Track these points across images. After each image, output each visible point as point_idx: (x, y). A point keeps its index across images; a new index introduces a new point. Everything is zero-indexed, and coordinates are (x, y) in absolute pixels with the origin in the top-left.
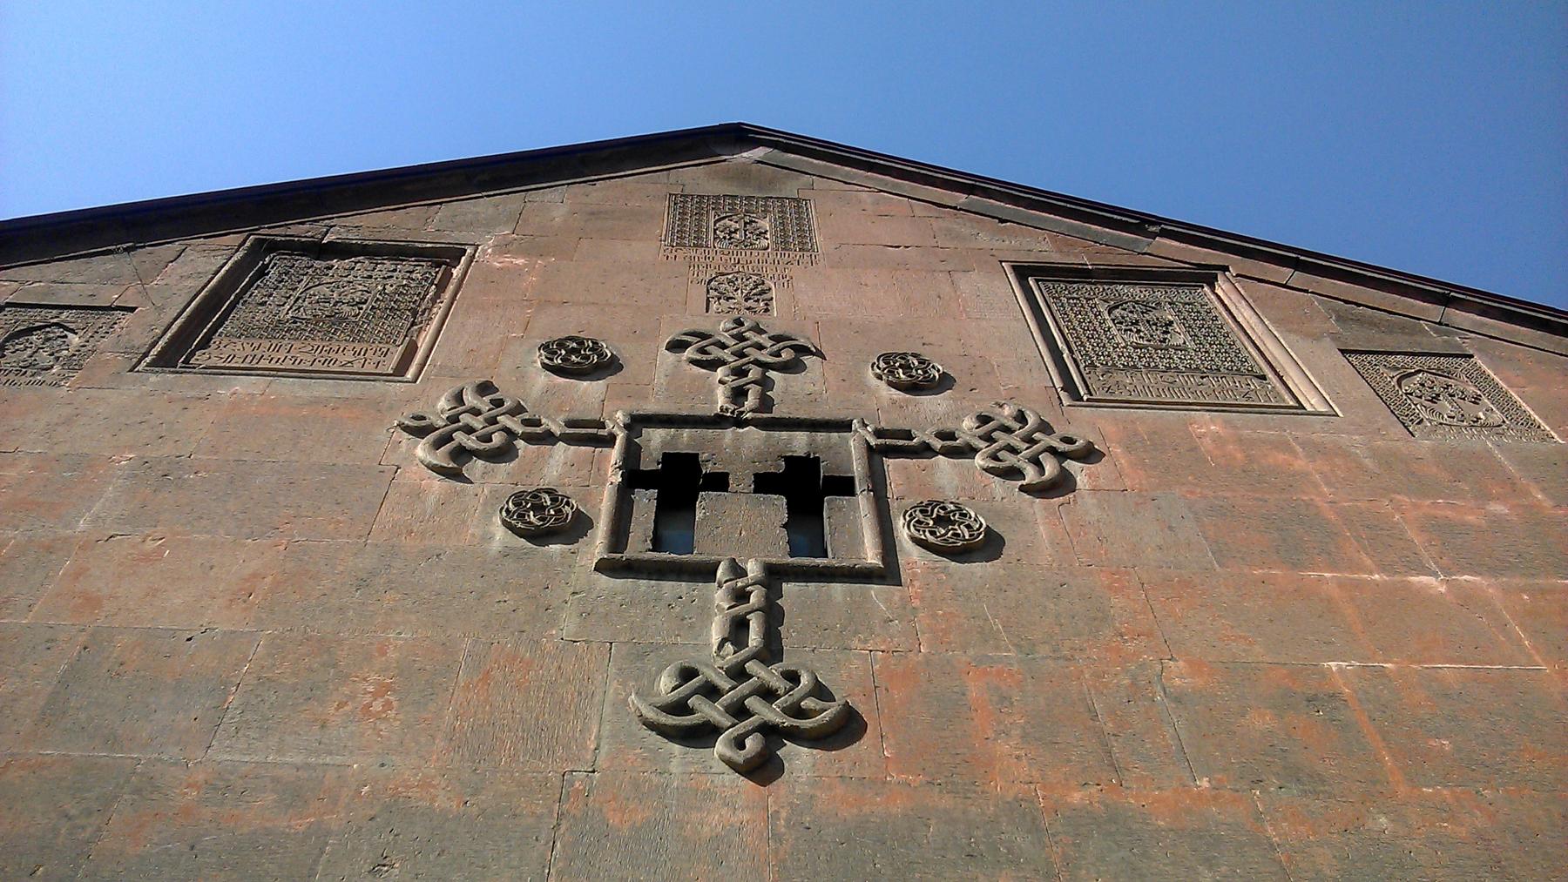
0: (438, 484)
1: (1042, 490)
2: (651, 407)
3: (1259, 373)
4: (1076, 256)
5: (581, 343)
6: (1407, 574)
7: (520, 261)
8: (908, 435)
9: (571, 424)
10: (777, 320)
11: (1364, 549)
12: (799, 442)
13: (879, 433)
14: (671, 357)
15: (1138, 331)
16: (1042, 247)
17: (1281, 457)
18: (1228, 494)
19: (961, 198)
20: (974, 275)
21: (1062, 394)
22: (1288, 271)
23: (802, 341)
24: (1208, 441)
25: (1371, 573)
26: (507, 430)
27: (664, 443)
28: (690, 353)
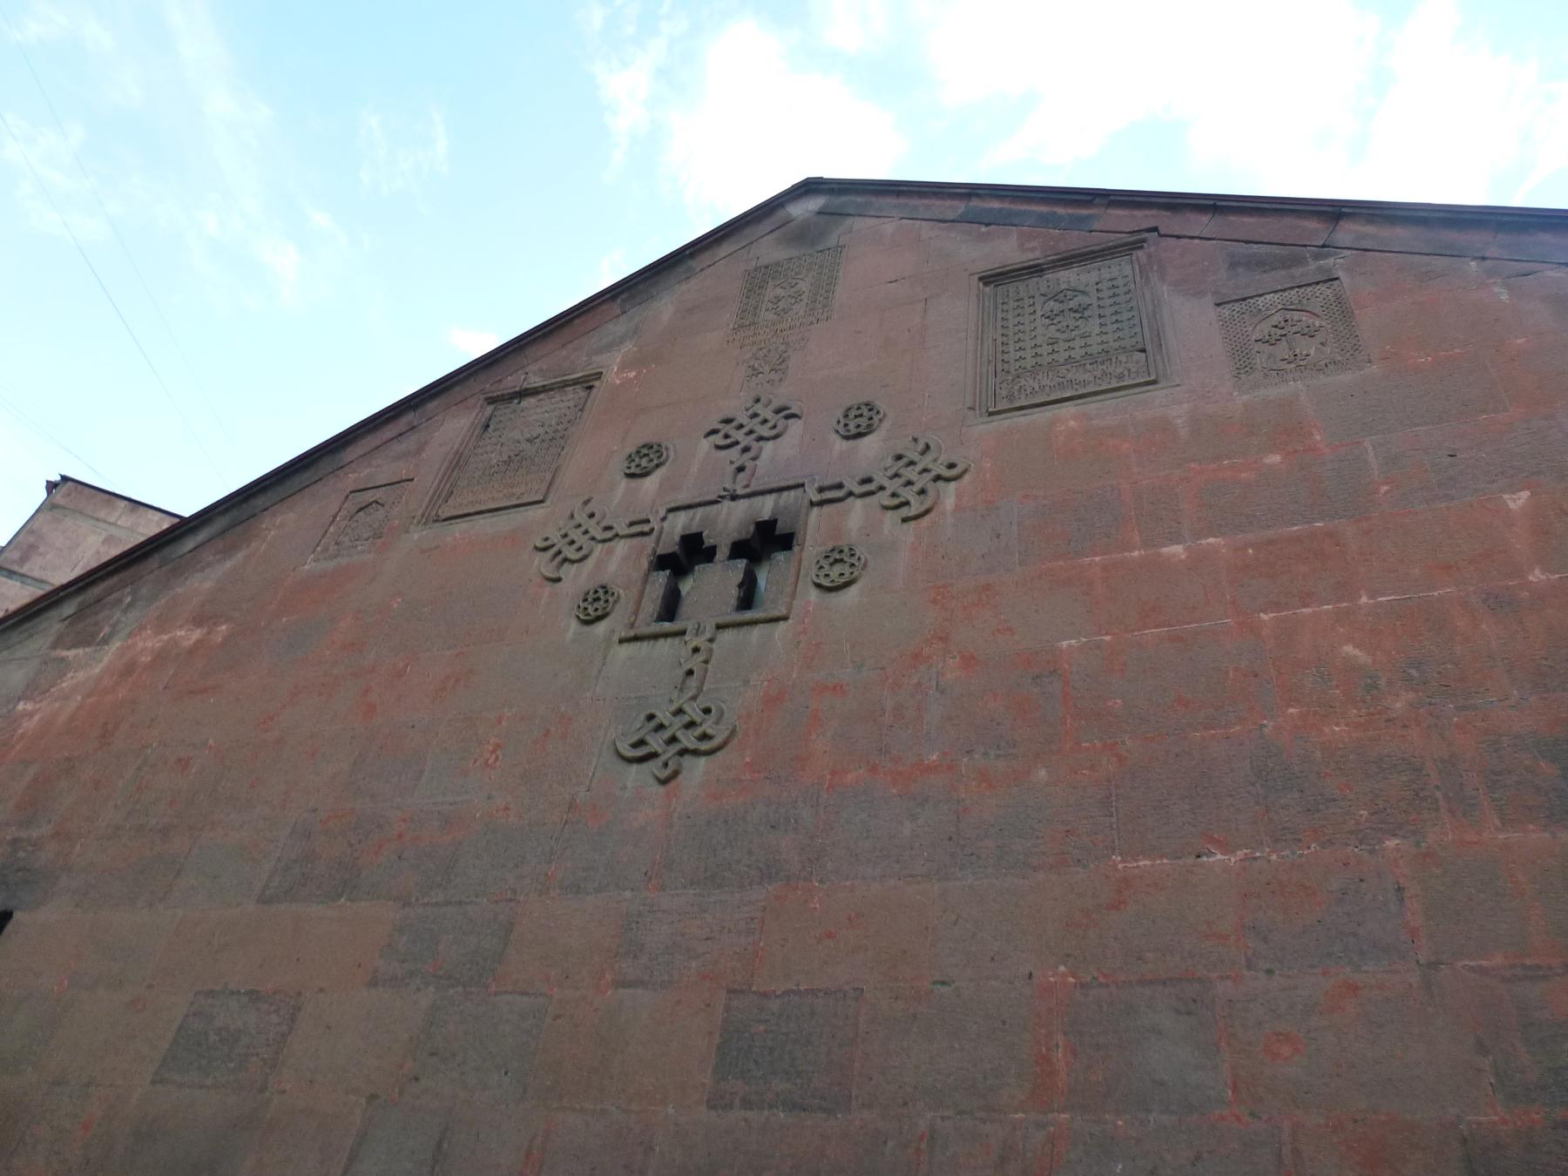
0: (549, 588)
2: (683, 498)
3: (1139, 346)
4: (1033, 249)
8: (840, 486)
9: (632, 524)
10: (783, 394)
12: (765, 507)
13: (821, 490)
14: (706, 445)
16: (1007, 249)
19: (960, 207)
22: (1205, 219)
23: (792, 411)
26: (593, 539)
27: (684, 528)
28: (718, 439)
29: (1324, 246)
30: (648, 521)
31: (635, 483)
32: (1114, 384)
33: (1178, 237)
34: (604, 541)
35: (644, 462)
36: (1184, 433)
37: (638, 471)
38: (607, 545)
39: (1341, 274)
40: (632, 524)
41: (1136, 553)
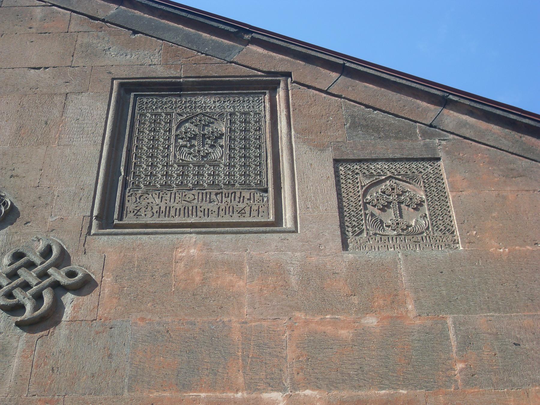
1: (28, 326)
6: (265, 390)
11: (244, 367)
15: (193, 146)
17: (229, 278)
18: (169, 319)
20: (84, 98)
21: (95, 222)
24: (182, 265)
25: (237, 391)
29: (431, 126)
32: (236, 219)
33: (309, 87)
36: (293, 280)
39: (441, 154)
41: (239, 395)
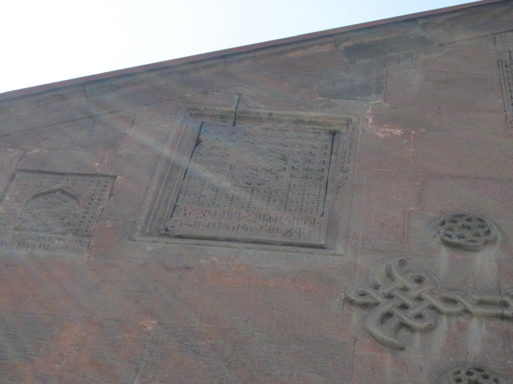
5: (469, 220)
7: (398, 132)
26: (433, 308)
30: (505, 305)
31: (460, 256)
34: (449, 315)
35: (468, 234)
37: (461, 241)
38: (454, 320)
40: (481, 303)
